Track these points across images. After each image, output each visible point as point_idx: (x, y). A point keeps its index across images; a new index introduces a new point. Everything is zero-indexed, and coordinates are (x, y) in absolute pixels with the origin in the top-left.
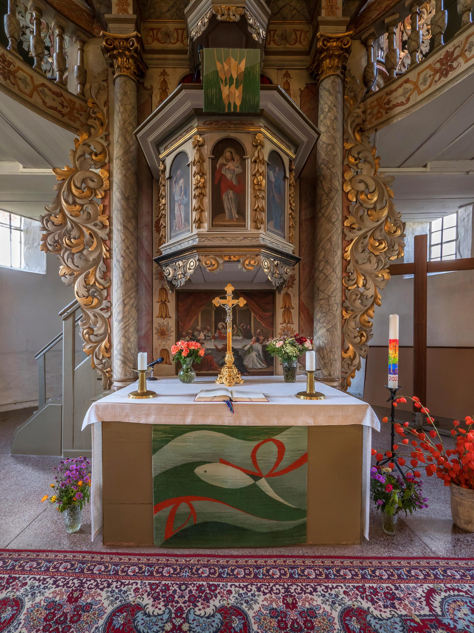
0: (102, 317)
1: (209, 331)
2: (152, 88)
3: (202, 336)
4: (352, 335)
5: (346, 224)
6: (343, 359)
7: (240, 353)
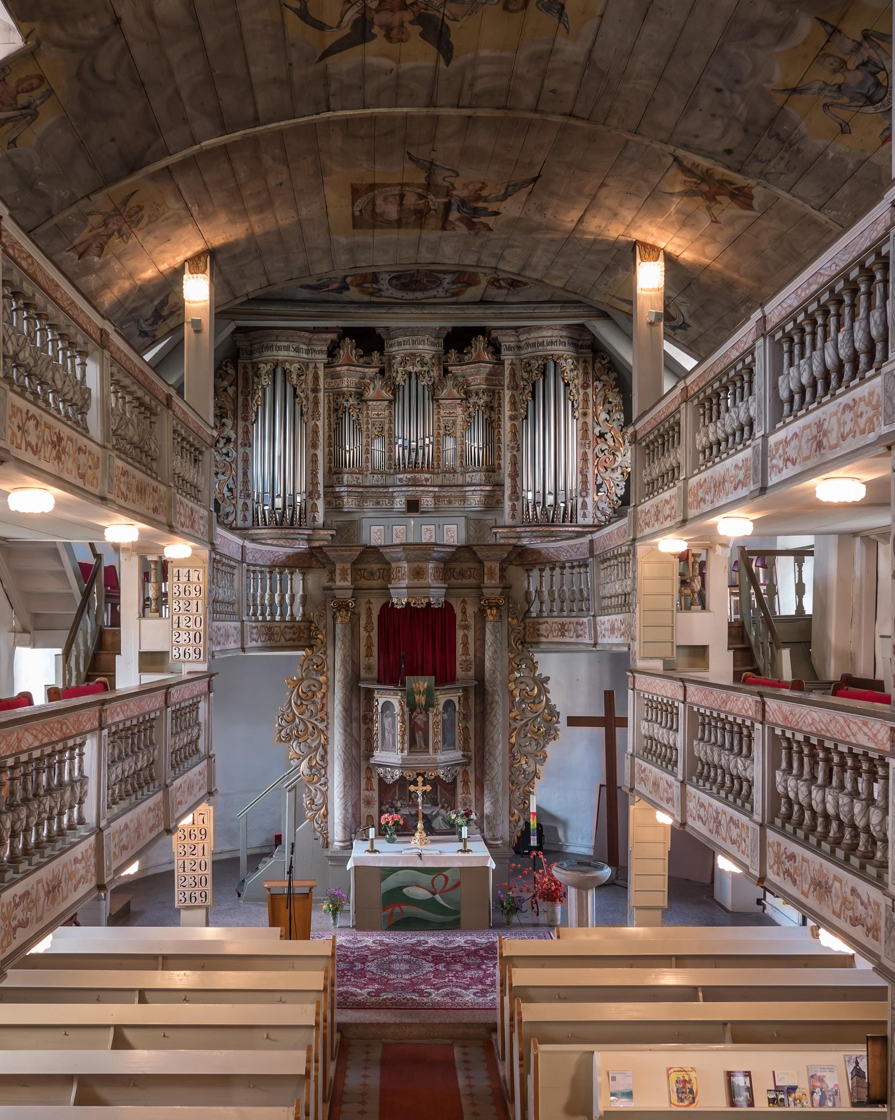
0: (321, 790)
1: (404, 800)
2: (359, 614)
3: (399, 804)
4: (517, 803)
5: (512, 715)
6: (510, 821)
7: (429, 817)
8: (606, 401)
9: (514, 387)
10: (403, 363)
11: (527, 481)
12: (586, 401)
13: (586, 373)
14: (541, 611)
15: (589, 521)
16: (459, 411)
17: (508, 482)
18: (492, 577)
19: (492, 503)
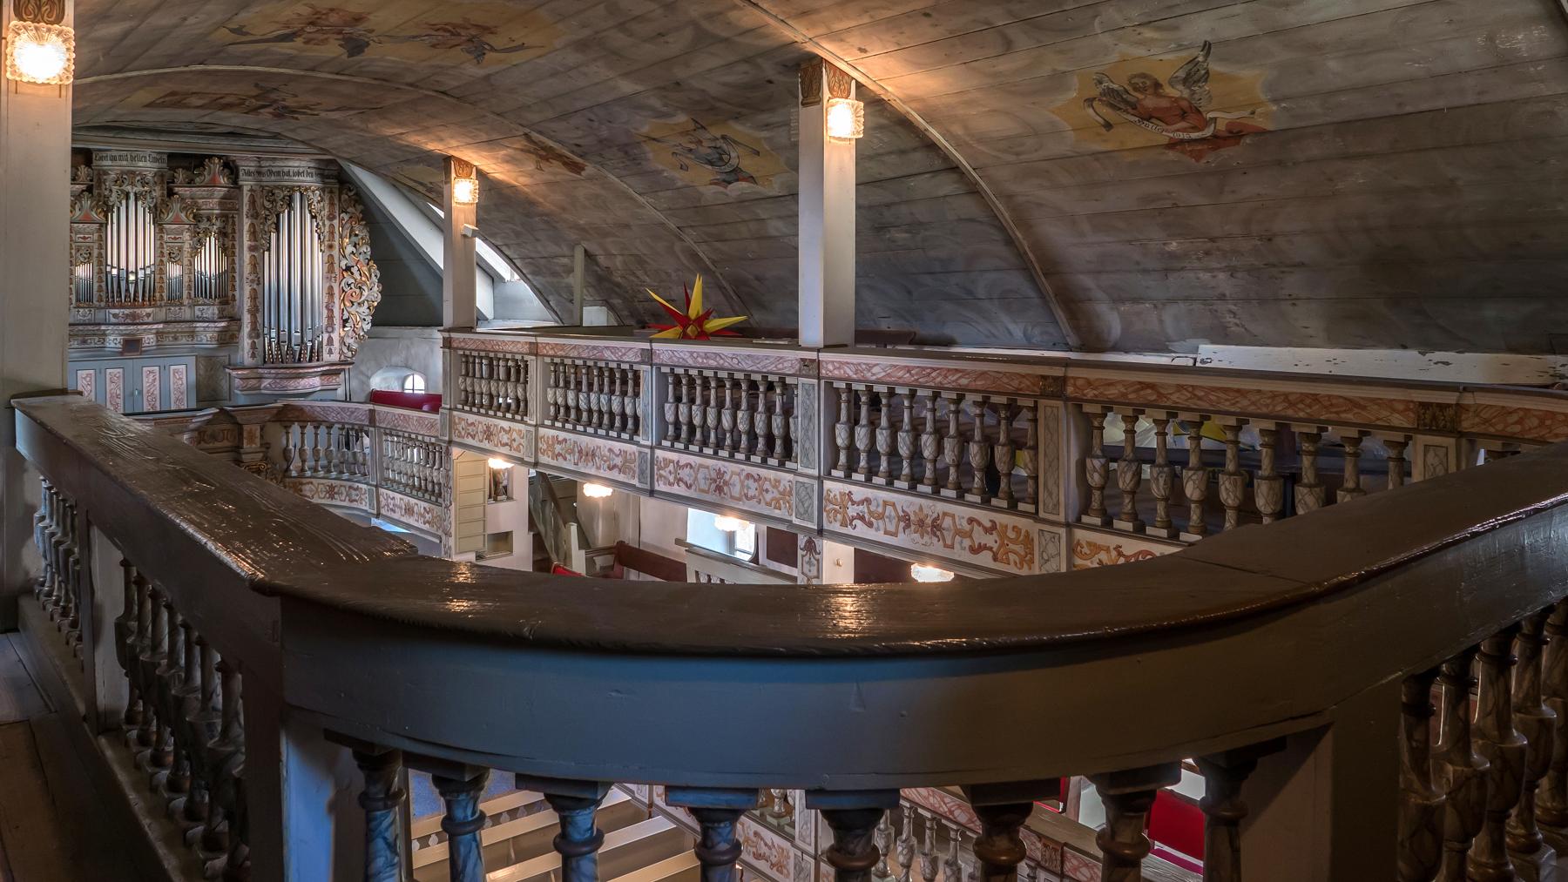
8: (352, 234)
9: (255, 215)
10: (119, 181)
11: (268, 316)
12: (332, 233)
13: (332, 204)
14: (303, 470)
15: (335, 357)
16: (187, 236)
17: (247, 318)
18: (251, 440)
19: (228, 338)
